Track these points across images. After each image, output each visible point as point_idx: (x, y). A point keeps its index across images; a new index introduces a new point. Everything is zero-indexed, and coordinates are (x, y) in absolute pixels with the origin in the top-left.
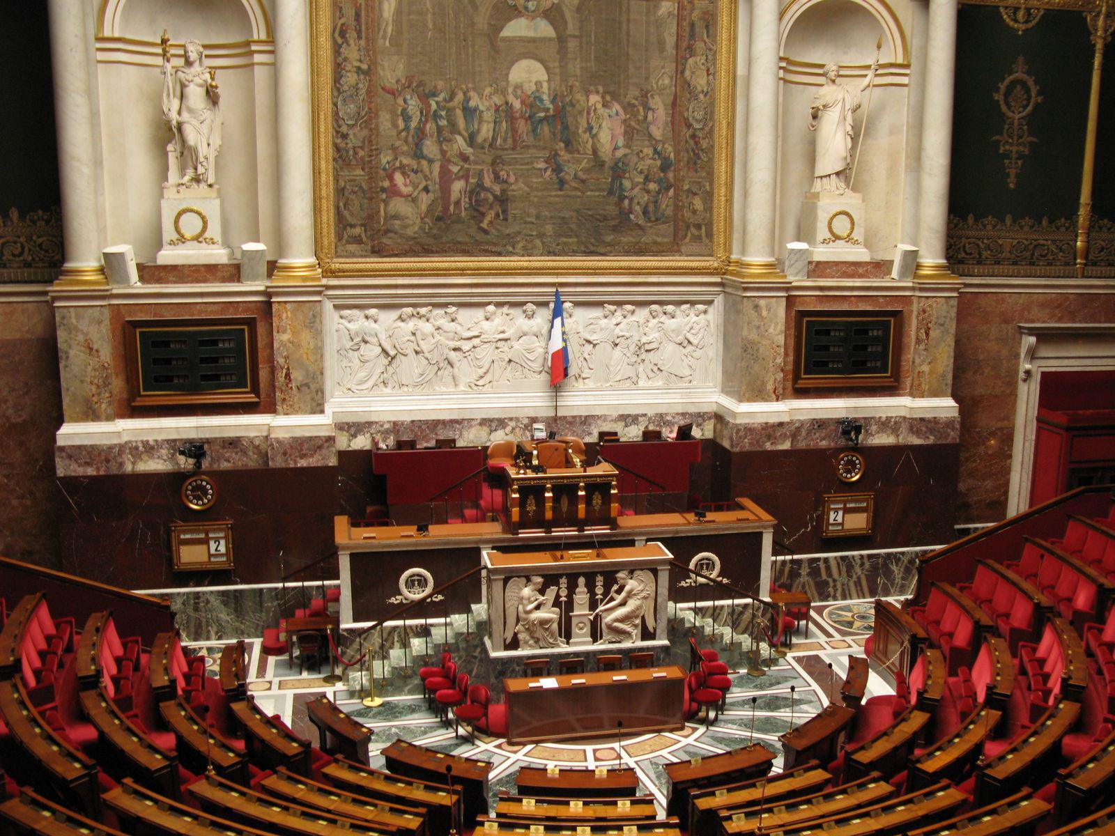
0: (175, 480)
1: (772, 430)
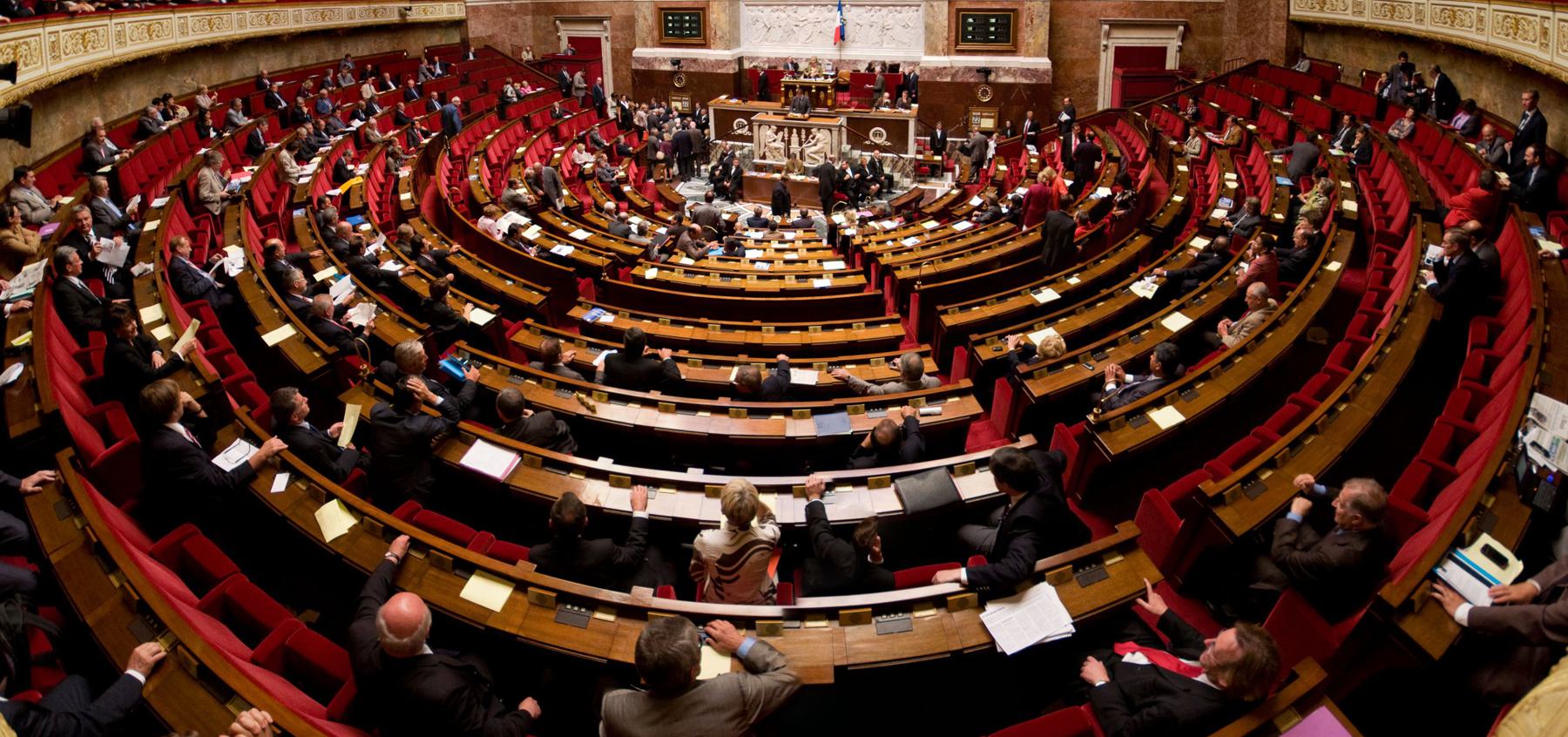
0: (672, 74)
1: (940, 71)
